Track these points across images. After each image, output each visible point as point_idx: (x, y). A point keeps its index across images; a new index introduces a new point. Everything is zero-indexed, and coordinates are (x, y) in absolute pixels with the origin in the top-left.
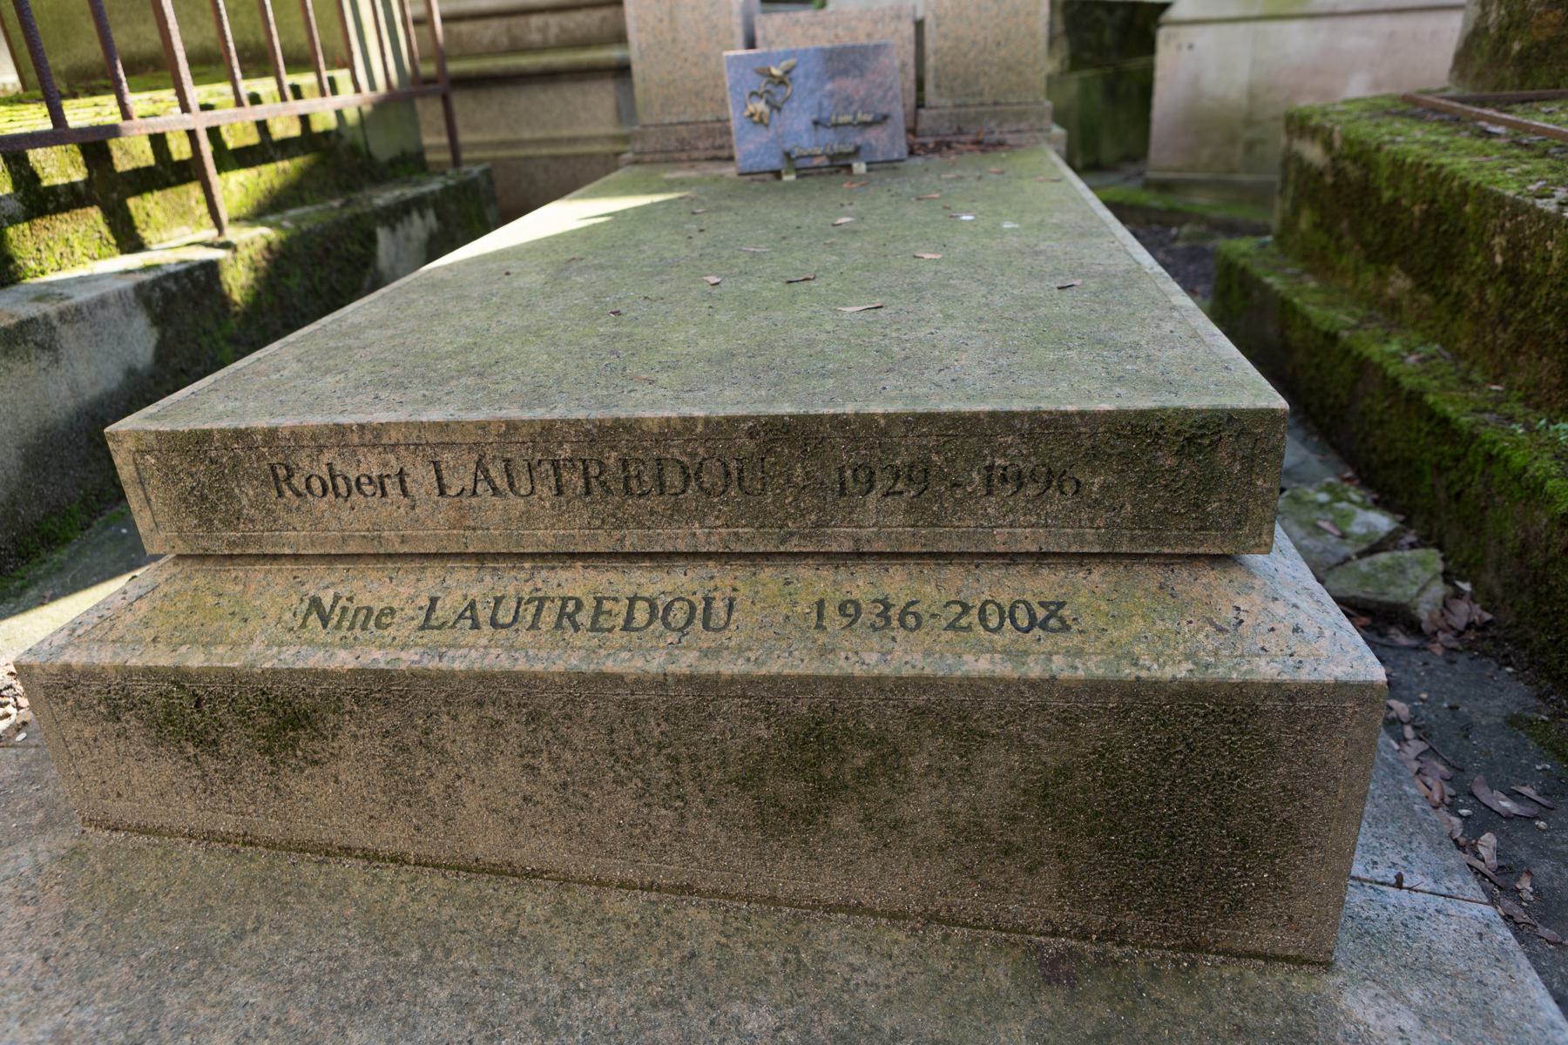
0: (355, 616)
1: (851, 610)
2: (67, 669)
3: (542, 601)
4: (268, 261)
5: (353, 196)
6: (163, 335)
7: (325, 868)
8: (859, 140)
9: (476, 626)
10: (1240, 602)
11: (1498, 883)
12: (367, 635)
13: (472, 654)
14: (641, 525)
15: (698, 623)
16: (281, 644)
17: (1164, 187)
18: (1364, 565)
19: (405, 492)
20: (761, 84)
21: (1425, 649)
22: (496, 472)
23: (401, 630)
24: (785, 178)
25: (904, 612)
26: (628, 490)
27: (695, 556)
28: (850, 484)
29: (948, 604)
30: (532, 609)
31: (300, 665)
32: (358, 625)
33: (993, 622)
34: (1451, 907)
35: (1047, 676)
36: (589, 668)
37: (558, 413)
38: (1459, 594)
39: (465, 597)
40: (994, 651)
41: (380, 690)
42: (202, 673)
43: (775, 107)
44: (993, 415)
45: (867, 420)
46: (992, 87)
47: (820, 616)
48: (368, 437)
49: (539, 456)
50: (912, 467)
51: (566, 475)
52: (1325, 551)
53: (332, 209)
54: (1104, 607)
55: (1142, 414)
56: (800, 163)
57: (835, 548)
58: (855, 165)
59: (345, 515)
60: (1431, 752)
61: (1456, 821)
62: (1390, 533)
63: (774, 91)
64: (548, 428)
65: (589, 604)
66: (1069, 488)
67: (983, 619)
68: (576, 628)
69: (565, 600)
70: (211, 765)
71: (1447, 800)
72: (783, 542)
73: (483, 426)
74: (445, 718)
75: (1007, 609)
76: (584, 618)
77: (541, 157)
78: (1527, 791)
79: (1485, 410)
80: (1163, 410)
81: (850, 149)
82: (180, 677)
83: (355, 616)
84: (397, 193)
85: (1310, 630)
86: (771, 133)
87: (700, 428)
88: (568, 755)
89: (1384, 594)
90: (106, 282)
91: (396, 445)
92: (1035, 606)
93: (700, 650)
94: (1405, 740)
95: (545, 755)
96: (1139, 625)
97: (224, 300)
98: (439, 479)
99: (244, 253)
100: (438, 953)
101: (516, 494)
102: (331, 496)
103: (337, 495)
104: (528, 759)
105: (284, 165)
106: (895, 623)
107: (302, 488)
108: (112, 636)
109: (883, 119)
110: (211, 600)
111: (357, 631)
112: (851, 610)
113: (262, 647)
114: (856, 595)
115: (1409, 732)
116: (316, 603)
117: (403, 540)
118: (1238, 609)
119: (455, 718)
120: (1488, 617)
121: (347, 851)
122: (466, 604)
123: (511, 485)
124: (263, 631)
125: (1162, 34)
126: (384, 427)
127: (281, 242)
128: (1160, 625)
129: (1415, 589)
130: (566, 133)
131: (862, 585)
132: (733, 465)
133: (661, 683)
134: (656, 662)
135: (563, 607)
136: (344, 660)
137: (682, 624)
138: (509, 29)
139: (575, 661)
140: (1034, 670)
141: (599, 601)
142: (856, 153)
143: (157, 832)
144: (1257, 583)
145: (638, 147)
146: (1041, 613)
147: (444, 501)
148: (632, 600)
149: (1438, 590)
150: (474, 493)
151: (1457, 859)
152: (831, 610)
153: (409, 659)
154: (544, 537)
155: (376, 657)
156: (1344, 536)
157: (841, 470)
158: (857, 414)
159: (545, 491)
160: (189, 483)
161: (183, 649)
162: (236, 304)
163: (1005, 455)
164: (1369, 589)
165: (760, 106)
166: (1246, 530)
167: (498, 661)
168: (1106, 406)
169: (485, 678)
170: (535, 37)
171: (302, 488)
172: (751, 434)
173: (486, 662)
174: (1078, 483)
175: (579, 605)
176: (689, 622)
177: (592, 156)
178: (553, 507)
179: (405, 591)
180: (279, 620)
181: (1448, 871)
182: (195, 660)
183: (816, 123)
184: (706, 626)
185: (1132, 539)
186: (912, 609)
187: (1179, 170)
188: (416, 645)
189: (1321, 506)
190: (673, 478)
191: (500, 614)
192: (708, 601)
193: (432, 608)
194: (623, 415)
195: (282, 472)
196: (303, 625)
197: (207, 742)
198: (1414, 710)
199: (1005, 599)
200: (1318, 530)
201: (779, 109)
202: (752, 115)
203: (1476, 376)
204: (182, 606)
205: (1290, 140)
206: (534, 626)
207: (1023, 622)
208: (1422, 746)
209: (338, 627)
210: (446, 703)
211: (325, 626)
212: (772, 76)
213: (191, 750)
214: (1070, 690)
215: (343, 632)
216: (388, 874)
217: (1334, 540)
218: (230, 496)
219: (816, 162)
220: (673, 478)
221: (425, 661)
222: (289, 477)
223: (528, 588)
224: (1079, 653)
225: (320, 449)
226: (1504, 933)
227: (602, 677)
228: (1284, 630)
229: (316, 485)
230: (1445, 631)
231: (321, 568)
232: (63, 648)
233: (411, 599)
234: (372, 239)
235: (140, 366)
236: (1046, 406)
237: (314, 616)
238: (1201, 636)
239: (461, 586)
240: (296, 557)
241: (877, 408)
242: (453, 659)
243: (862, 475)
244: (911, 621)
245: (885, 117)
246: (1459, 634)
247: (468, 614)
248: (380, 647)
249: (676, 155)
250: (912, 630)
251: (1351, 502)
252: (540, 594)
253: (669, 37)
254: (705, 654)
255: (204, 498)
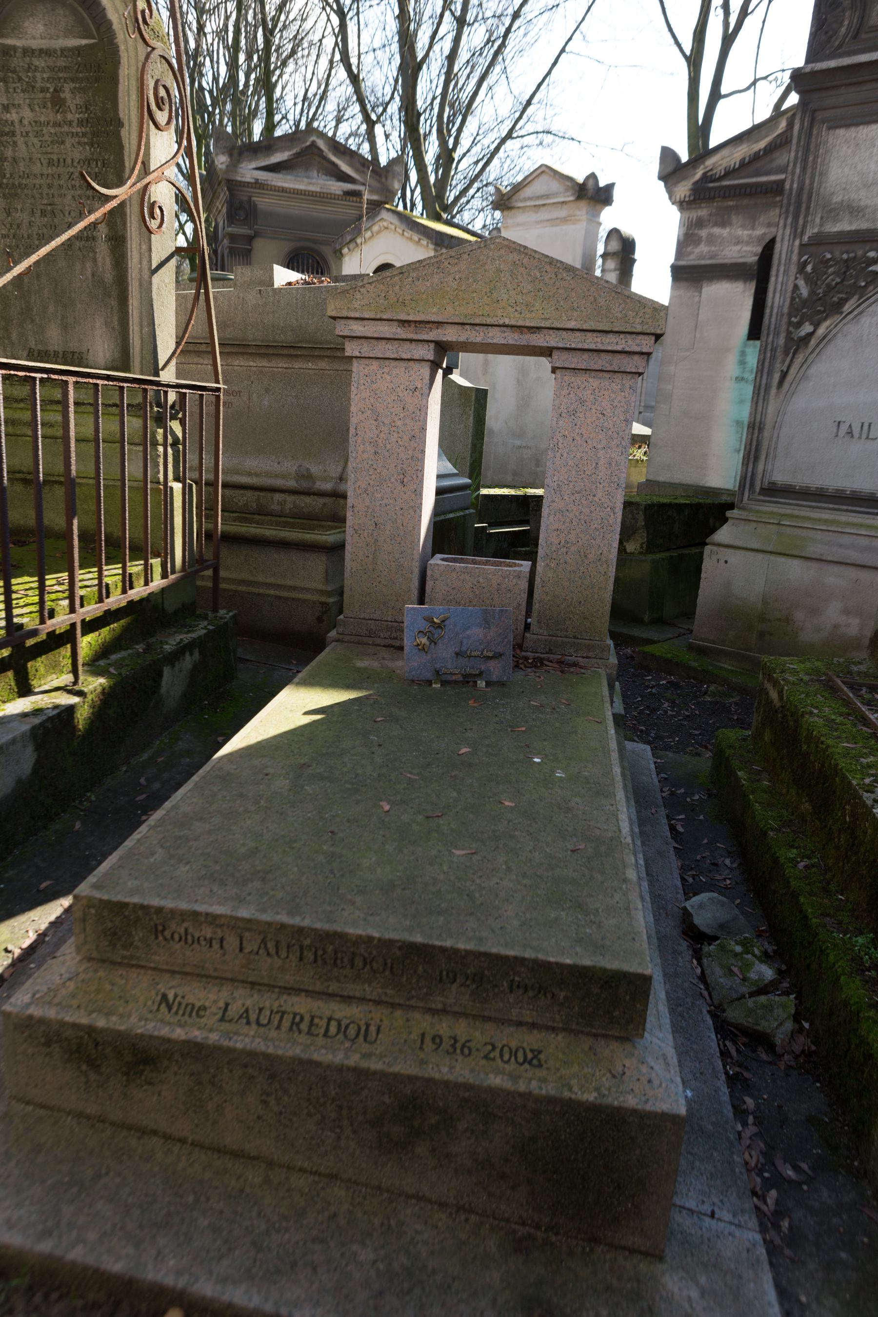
0: (186, 1008)
1: (438, 1041)
2: (31, 1017)
3: (283, 1013)
4: (101, 700)
5: (152, 640)
6: (39, 756)
7: (142, 1141)
8: (483, 667)
9: (248, 1023)
10: (627, 1062)
11: (767, 1222)
12: (190, 1021)
13: (246, 1040)
14: (338, 981)
15: (361, 1038)
16: (146, 1020)
17: (702, 651)
18: (750, 1003)
19: (222, 947)
20: (424, 626)
21: (775, 1064)
22: (271, 946)
23: (210, 1020)
24: (434, 686)
25: (463, 1046)
26: (335, 963)
27: (363, 1000)
28: (444, 977)
29: (486, 1044)
30: (278, 1017)
31: (156, 1033)
32: (187, 1014)
33: (506, 1057)
34: (738, 1233)
35: (527, 1091)
36: (305, 1056)
37: (306, 923)
38: (801, 1030)
39: (243, 1005)
40: (503, 1073)
41: (195, 1051)
42: (103, 1030)
43: (432, 641)
44: (516, 958)
45: (456, 951)
46: (574, 628)
47: (422, 1042)
48: (209, 919)
49: (294, 941)
50: (475, 975)
51: (305, 953)
52: (731, 988)
53: (138, 654)
54: (561, 1056)
55: (584, 968)
56: (444, 678)
57: (433, 1006)
58: (479, 682)
59: (188, 953)
60: (759, 1135)
61: (759, 1180)
62: (772, 981)
63: (434, 631)
64: (301, 930)
65: (307, 1019)
66: (549, 995)
67: (501, 1056)
68: (300, 1032)
69: (295, 1014)
70: (93, 1077)
71: (759, 1166)
72: (409, 999)
73: (269, 924)
74: (226, 1071)
75: (514, 1051)
76: (304, 1026)
77: (269, 595)
78: (804, 1166)
79: (828, 915)
80: (594, 967)
81: (477, 672)
82: (91, 1030)
83: (186, 1008)
84: (178, 638)
85: (656, 1083)
86: (429, 657)
87: (375, 942)
88: (286, 1098)
89: (757, 1024)
90: (14, 724)
91: (223, 925)
92: (528, 1051)
93: (361, 1053)
94: (747, 1124)
95: (273, 1096)
96: (576, 1068)
97: (74, 728)
98: (241, 943)
99: (90, 697)
100: (203, 1199)
101: (279, 957)
102: (182, 943)
103: (186, 942)
104: (264, 1097)
105: (114, 625)
106: (458, 1051)
107: (169, 937)
108: (56, 1001)
109: (498, 656)
110: (108, 987)
111: (186, 1017)
112: (438, 1041)
113: (136, 1020)
114: (441, 1032)
115: (751, 1119)
116: (164, 997)
117: (216, 970)
118: (624, 1066)
119: (231, 1071)
120: (813, 1048)
121: (155, 1133)
122: (244, 1009)
123: (277, 953)
124: (137, 1010)
125: (707, 549)
126: (219, 916)
127: (110, 687)
128: (586, 1070)
129: (776, 1024)
130: (289, 582)
131: (444, 1027)
132: (389, 961)
133: (340, 1069)
134: (338, 1058)
135: (294, 1018)
136: (179, 1034)
137: (353, 1037)
138: (258, 499)
139: (296, 1051)
140: (522, 1087)
141: (313, 1018)
142: (480, 675)
143: (50, 1108)
144: (636, 1052)
145: (341, 630)
146: (530, 1055)
147: (241, 955)
148: (330, 1019)
149: (789, 1025)
150: (257, 953)
151: (750, 1203)
152: (428, 1040)
153: (214, 1037)
154: (289, 979)
155: (197, 1035)
156: (744, 979)
157: (441, 972)
158: (452, 948)
159: (294, 958)
160: (110, 925)
161: (94, 1015)
162: (80, 731)
163: (519, 976)
164: (750, 1020)
165: (424, 640)
166: (632, 1026)
167: (259, 1045)
168: (568, 961)
169: (252, 1054)
170: (276, 507)
171: (169, 937)
172: (400, 948)
173: (253, 1046)
174: (553, 994)
175: (302, 1019)
176: (357, 1035)
177: (305, 601)
178: (296, 966)
179: (212, 996)
180: (145, 1005)
181: (743, 1211)
182: (101, 1023)
183: (457, 654)
184: (365, 1040)
185: (578, 1023)
186: (468, 1044)
187: (714, 642)
188: (217, 1030)
189: (736, 955)
190: (359, 962)
191: (261, 1018)
192: (368, 1026)
193: (226, 1010)
194: (339, 930)
195: (160, 928)
196: (158, 1010)
197: (94, 1065)
198: (757, 1106)
199: (513, 1045)
200: (731, 973)
201: (435, 643)
202: (418, 645)
203: (832, 887)
204: (93, 988)
205: (764, 678)
206: (278, 1027)
207: (521, 1060)
208: (755, 1130)
209: (176, 1013)
210: (228, 1063)
211: (170, 1011)
212: (435, 623)
213: (84, 1067)
214: (538, 1099)
215: (179, 1017)
216: (176, 1149)
217: (738, 981)
218: (130, 935)
219: (454, 678)
220: (359, 962)
221: (222, 1040)
222: (164, 929)
223: (276, 1004)
224: (543, 1080)
225: (183, 921)
226: (762, 1251)
227: (311, 1062)
228: (644, 1080)
229: (177, 937)
230: (789, 1054)
231: (167, 976)
232: (29, 1005)
233: (215, 1002)
234: (160, 675)
235: (24, 777)
236: (541, 957)
237: (163, 1005)
238: (604, 1079)
239: (242, 999)
240: (154, 969)
241: (461, 946)
242: (236, 1041)
243: (451, 975)
244: (466, 1051)
245: (501, 655)
246: (797, 1057)
247: (245, 1015)
248: (199, 1028)
249: (365, 639)
250: (466, 1056)
251: (754, 955)
252: (283, 1009)
253: (371, 567)
254: (365, 1056)
255: (115, 934)
